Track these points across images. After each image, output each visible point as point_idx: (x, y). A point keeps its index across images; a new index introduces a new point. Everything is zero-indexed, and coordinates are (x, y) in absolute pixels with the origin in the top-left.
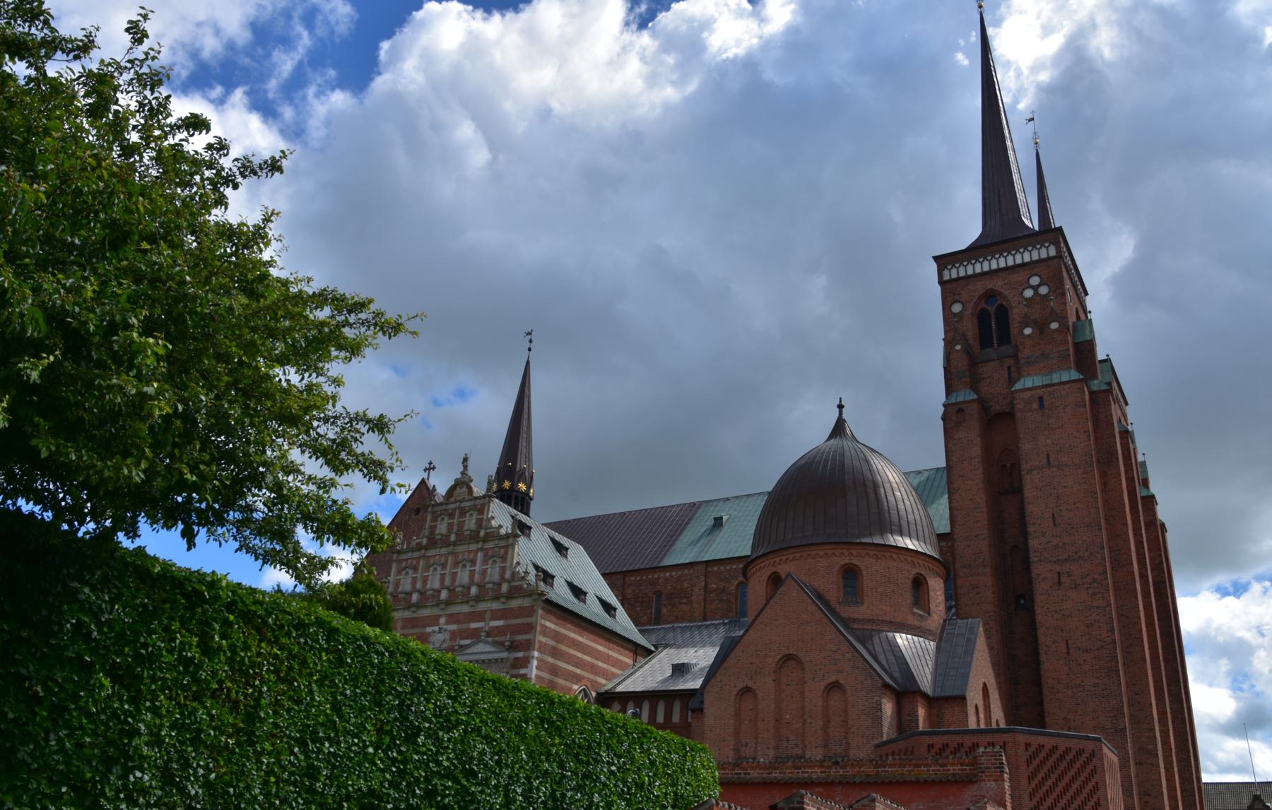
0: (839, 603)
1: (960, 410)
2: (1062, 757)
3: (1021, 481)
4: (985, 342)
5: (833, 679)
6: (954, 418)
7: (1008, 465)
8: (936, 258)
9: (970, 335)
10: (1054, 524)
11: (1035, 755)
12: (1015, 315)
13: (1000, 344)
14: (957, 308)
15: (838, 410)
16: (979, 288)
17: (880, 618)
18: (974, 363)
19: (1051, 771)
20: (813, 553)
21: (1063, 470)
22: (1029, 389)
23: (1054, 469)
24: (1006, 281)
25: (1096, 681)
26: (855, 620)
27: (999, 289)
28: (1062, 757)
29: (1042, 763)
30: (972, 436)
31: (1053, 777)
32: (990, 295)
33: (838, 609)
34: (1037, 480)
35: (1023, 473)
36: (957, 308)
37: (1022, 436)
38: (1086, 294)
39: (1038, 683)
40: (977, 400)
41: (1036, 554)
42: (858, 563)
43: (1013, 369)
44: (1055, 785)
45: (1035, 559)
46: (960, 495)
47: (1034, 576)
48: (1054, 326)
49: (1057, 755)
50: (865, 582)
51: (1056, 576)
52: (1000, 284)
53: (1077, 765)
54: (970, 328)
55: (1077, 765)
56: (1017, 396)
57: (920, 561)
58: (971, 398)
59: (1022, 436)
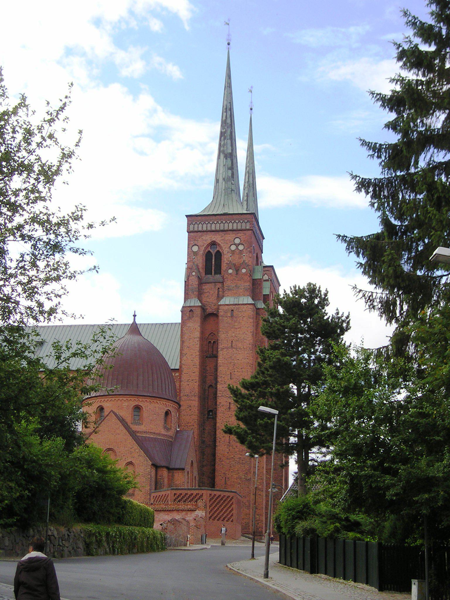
0: (132, 424)
1: (191, 311)
2: (222, 499)
3: (217, 351)
4: (208, 271)
5: (129, 460)
6: (188, 314)
7: (212, 342)
8: (187, 216)
9: (200, 266)
10: (231, 379)
11: (213, 498)
12: (226, 258)
13: (215, 273)
14: (195, 249)
15: (133, 317)
16: (208, 238)
17: (149, 431)
18: (201, 283)
19: (217, 504)
20: (121, 399)
21: (238, 351)
22: (227, 305)
23: (233, 349)
24: (223, 238)
25: (240, 456)
26: (138, 432)
27: (219, 242)
28: (222, 499)
29: (215, 501)
30: (195, 325)
31: (218, 506)
32: (213, 244)
33: (132, 426)
34: (225, 355)
35: (219, 350)
36: (195, 249)
37: (221, 330)
38: (264, 238)
39: (214, 455)
40: (201, 306)
41: (221, 392)
42: (141, 405)
43: (220, 290)
44: (218, 509)
45: (220, 395)
46: (187, 357)
47: (218, 403)
48: (244, 271)
49: (220, 498)
50: (144, 414)
51: (229, 404)
52: (219, 239)
53: (226, 502)
54: (200, 261)
55: (226, 502)
56: (221, 307)
57: (169, 404)
58: (198, 305)
59: (221, 330)
